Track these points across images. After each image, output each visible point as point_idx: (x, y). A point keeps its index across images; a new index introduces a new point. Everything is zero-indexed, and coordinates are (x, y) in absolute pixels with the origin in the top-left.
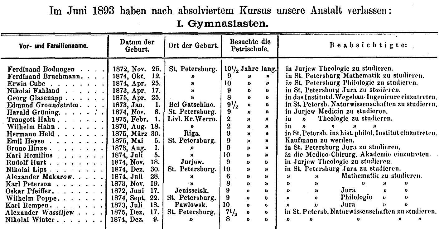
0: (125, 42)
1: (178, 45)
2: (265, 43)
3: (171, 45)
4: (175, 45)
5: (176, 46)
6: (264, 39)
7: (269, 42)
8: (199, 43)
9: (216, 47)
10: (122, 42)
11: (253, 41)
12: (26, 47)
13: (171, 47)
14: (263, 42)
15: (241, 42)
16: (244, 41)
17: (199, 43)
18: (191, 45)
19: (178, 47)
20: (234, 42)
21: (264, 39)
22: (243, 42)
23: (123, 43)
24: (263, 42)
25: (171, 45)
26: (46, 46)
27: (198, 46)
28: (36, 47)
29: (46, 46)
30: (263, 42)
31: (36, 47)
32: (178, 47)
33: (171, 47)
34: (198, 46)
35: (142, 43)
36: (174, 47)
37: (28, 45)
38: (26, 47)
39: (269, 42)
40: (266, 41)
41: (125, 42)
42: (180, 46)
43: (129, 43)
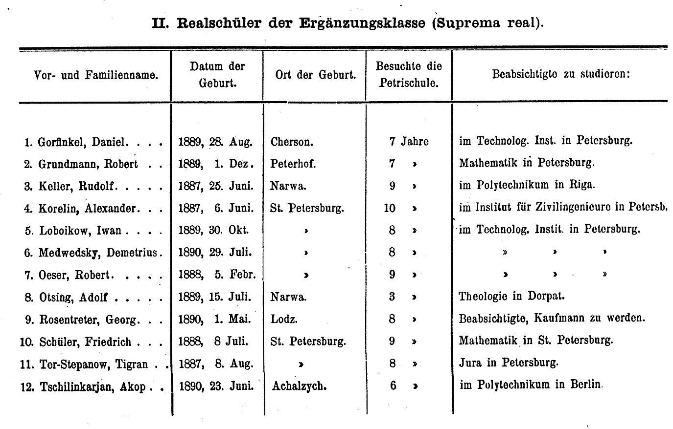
0: (199, 67)
1: (289, 73)
2: (433, 68)
3: (279, 73)
4: (285, 74)
5: (287, 76)
6: (431, 62)
7: (439, 67)
8: (325, 71)
9: (351, 78)
10: (195, 66)
11: (413, 64)
12: (47, 76)
13: (279, 76)
14: (430, 66)
15: (394, 66)
16: (398, 65)
17: (325, 71)
18: (311, 74)
19: (290, 77)
20: (383, 66)
21: (431, 62)
22: (397, 66)
23: (195, 68)
24: (430, 66)
25: (279, 73)
26: (83, 75)
27: (323, 75)
28: (64, 76)
29: (83, 75)
30: (430, 66)
31: (64, 76)
32: (290, 77)
33: (279, 76)
34: (323, 75)
35: (225, 67)
36: (285, 78)
37: (51, 74)
38: (47, 76)
39: (439, 67)
40: (435, 65)
41: (199, 67)
42: (294, 75)
43: (205, 67)
